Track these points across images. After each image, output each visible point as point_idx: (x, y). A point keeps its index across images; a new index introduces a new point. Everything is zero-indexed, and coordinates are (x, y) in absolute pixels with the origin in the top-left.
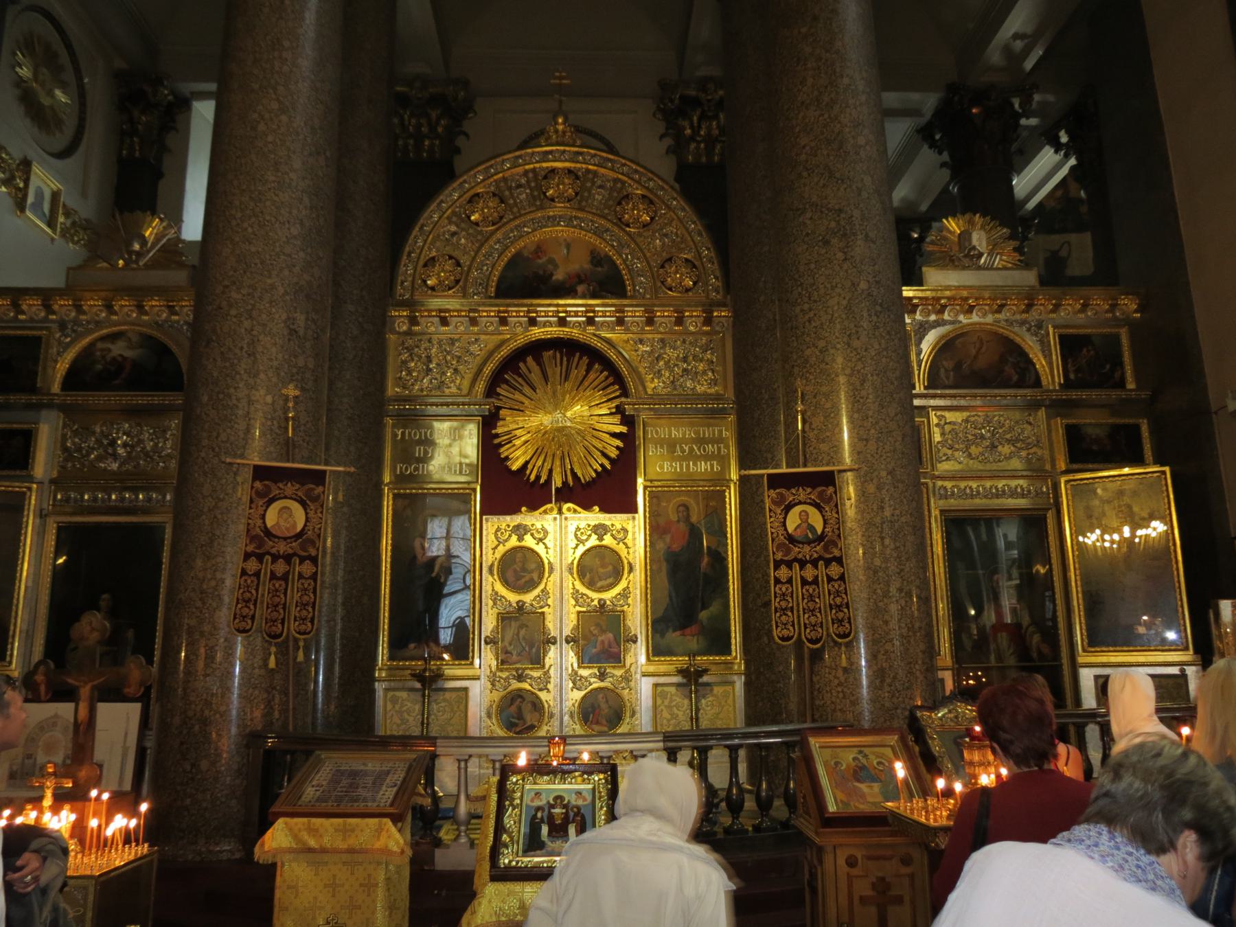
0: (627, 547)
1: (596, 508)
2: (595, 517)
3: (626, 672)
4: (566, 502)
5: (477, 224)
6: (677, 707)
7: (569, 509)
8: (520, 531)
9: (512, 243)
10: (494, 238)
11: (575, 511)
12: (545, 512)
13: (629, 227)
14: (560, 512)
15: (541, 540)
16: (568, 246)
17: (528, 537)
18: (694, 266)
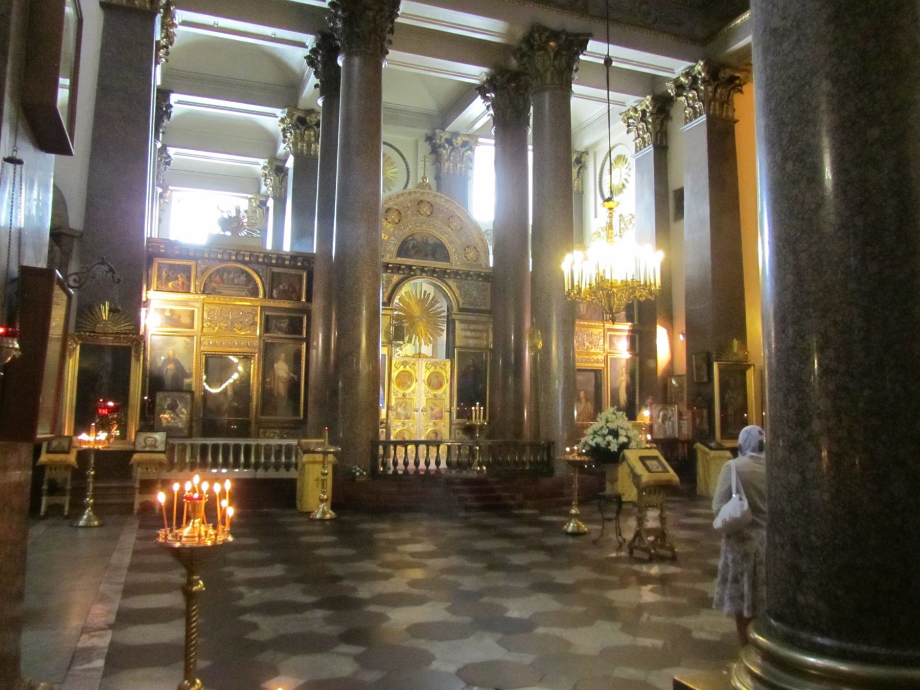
17: (407, 367)
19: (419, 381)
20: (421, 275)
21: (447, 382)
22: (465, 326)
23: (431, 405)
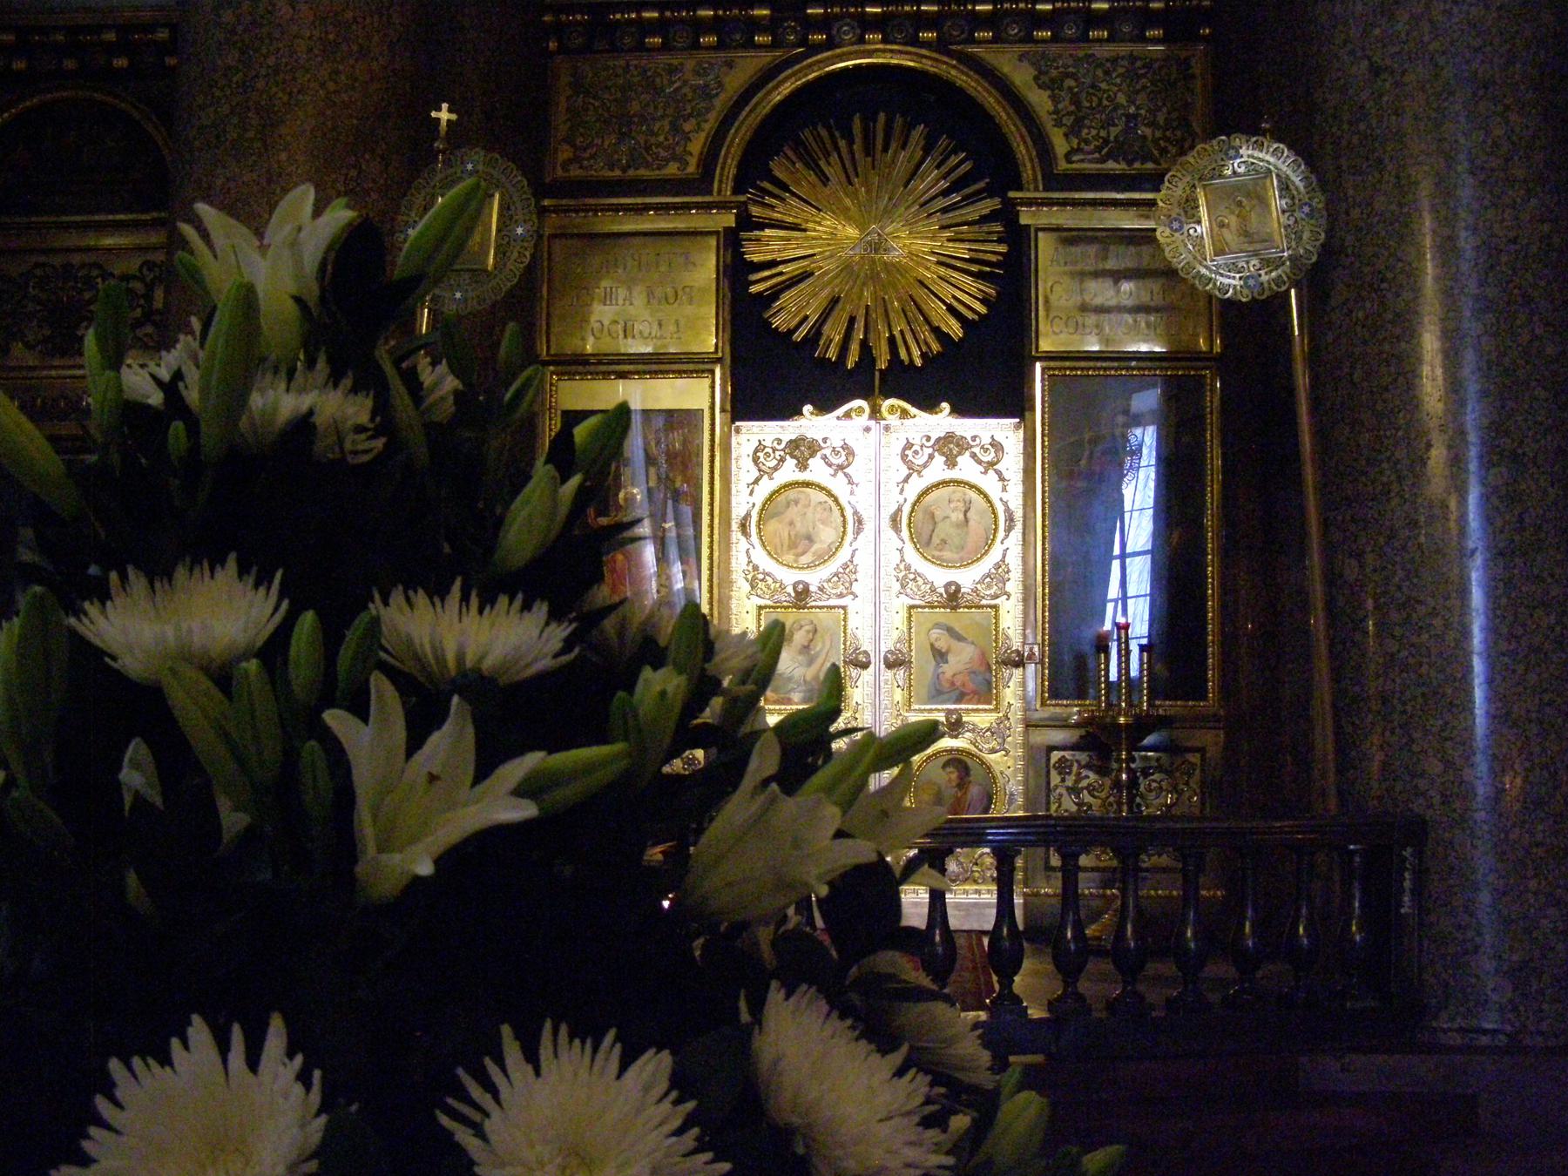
0: (1002, 479)
2: (943, 421)
3: (1000, 722)
4: (887, 397)
6: (1091, 789)
7: (892, 410)
8: (802, 450)
11: (905, 414)
12: (847, 415)
19: (869, 527)
20: (861, 40)
21: (1009, 529)
22: (1087, 255)
23: (935, 633)
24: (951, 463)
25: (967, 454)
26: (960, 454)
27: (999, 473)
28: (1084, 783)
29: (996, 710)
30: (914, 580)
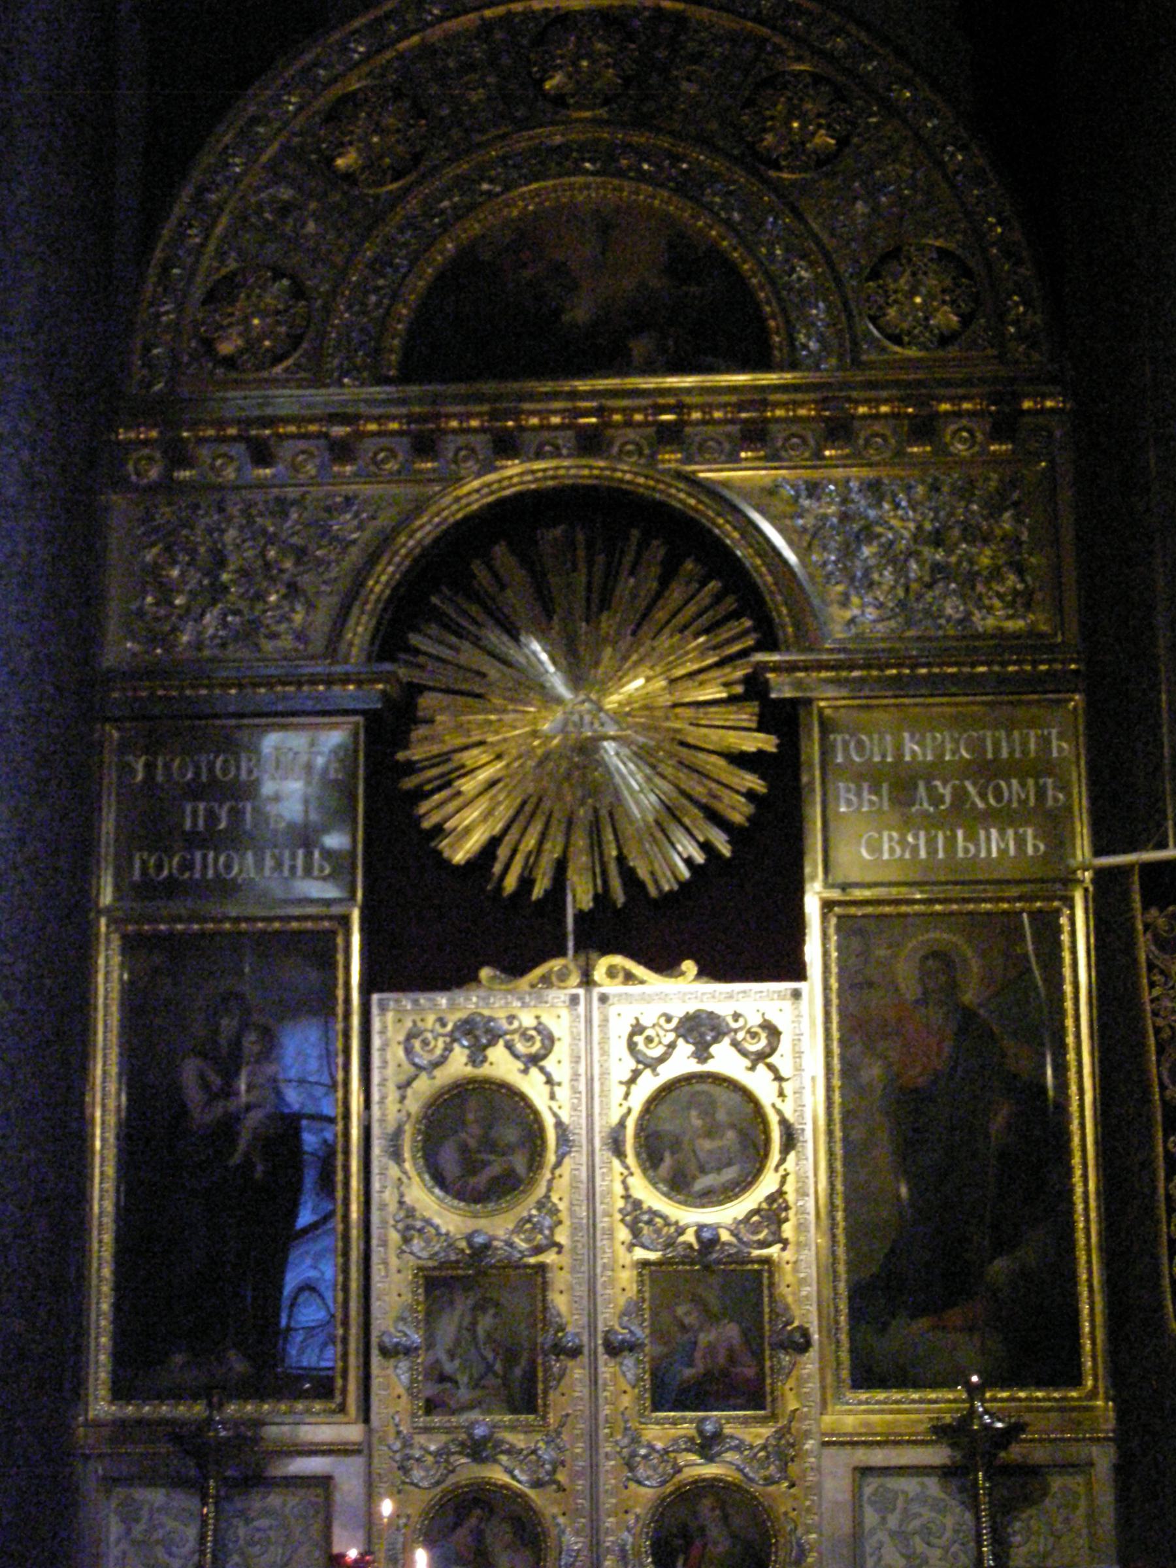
1: (689, 967)
3: (781, 1434)
4: (605, 951)
5: (349, 177)
6: (926, 1532)
7: (611, 973)
9: (445, 227)
10: (397, 217)
11: (629, 977)
12: (546, 980)
13: (779, 168)
14: (587, 981)
15: (534, 1060)
16: (605, 228)
18: (968, 273)
24: (702, 1054)
25: (727, 1041)
26: (716, 1040)
27: (771, 1067)
28: (916, 1524)
29: (774, 1417)
30: (649, 1222)
